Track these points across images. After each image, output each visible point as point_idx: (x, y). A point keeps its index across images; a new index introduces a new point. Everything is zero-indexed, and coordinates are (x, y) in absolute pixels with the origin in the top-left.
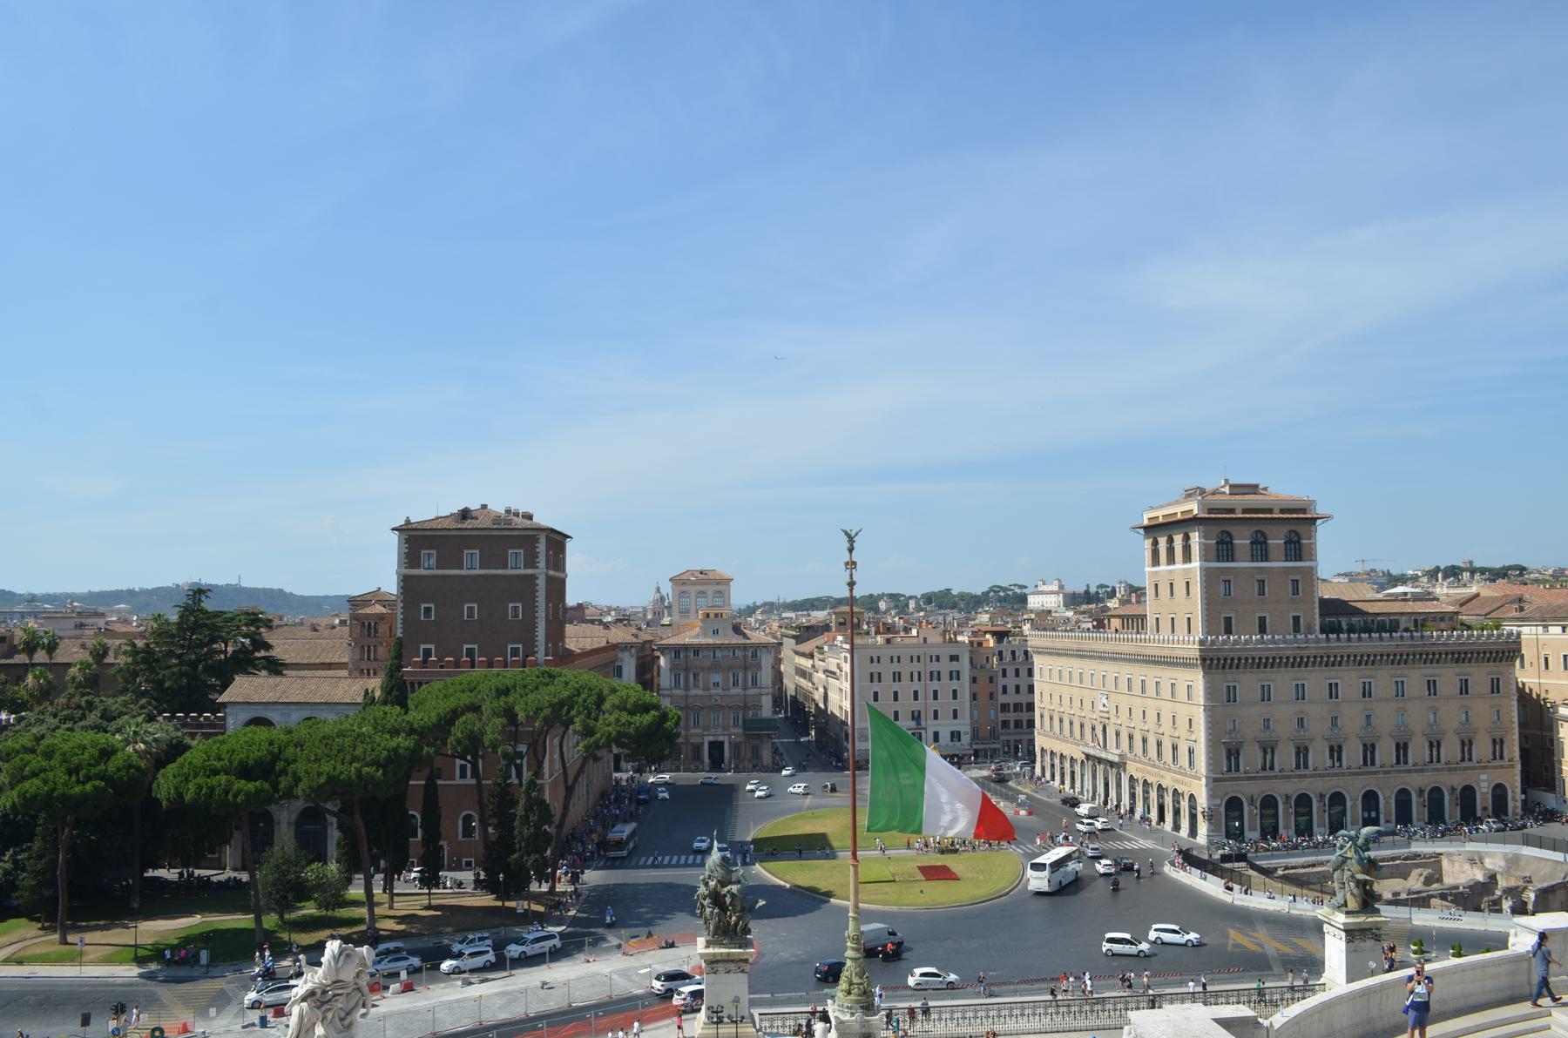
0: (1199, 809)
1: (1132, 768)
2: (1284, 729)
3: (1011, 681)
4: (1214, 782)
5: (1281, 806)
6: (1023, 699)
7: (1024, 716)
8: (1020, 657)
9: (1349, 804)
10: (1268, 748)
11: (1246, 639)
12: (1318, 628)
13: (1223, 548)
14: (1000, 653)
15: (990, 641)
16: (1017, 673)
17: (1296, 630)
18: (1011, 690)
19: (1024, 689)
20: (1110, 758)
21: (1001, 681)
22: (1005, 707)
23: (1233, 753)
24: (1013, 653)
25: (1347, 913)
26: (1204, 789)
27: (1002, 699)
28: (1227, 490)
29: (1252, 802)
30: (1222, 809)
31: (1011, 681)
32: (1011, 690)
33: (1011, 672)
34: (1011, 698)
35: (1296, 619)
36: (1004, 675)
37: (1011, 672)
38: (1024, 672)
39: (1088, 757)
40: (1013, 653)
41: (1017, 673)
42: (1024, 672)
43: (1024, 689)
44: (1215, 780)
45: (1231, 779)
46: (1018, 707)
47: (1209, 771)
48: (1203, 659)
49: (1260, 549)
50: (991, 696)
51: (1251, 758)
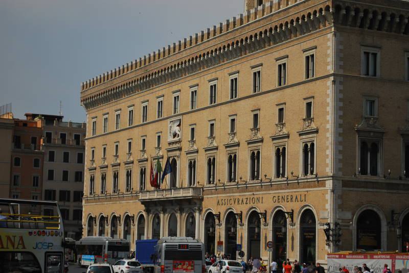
0: (320, 229)
1: (211, 204)
3: (58, 166)
4: (344, 185)
6: (70, 186)
7: (71, 206)
8: (70, 140)
14: (49, 135)
15: (39, 123)
16: (66, 158)
18: (58, 175)
19: (71, 177)
20: (181, 194)
21: (47, 165)
22: (50, 194)
24: (63, 136)
26: (329, 197)
27: (47, 185)
29: (391, 223)
31: (58, 166)
32: (58, 175)
33: (59, 155)
34: (57, 185)
36: (52, 158)
37: (59, 155)
38: (73, 157)
39: (148, 204)
40: (63, 136)
41: (66, 158)
42: (73, 157)
43: (71, 177)
44: (346, 184)
45: (366, 184)
46: (64, 195)
47: (337, 169)
50: (36, 182)
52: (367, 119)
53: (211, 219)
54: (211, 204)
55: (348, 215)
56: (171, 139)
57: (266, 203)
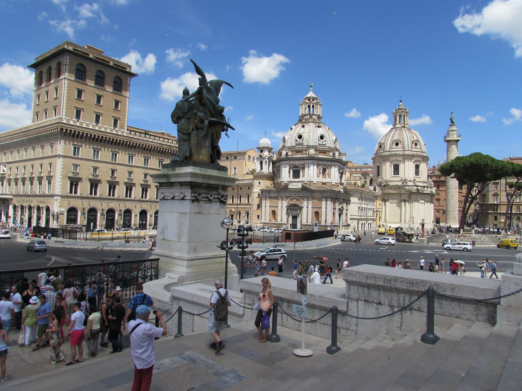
2: (104, 174)
5: (99, 215)
9: (133, 216)
10: (94, 184)
11: (87, 123)
12: (126, 128)
13: (80, 74)
17: (115, 125)
23: (74, 182)
25: (195, 164)
28: (86, 47)
30: (66, 214)
35: (116, 121)
48: (62, 129)
49: (100, 81)
51: (84, 188)
52: (73, 173)
53: (15, 207)
54: (16, 201)
55: (63, 209)
56: (2, 172)
57: (34, 203)
